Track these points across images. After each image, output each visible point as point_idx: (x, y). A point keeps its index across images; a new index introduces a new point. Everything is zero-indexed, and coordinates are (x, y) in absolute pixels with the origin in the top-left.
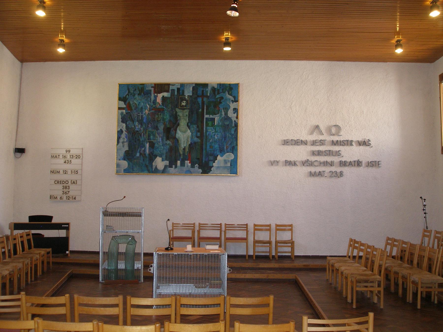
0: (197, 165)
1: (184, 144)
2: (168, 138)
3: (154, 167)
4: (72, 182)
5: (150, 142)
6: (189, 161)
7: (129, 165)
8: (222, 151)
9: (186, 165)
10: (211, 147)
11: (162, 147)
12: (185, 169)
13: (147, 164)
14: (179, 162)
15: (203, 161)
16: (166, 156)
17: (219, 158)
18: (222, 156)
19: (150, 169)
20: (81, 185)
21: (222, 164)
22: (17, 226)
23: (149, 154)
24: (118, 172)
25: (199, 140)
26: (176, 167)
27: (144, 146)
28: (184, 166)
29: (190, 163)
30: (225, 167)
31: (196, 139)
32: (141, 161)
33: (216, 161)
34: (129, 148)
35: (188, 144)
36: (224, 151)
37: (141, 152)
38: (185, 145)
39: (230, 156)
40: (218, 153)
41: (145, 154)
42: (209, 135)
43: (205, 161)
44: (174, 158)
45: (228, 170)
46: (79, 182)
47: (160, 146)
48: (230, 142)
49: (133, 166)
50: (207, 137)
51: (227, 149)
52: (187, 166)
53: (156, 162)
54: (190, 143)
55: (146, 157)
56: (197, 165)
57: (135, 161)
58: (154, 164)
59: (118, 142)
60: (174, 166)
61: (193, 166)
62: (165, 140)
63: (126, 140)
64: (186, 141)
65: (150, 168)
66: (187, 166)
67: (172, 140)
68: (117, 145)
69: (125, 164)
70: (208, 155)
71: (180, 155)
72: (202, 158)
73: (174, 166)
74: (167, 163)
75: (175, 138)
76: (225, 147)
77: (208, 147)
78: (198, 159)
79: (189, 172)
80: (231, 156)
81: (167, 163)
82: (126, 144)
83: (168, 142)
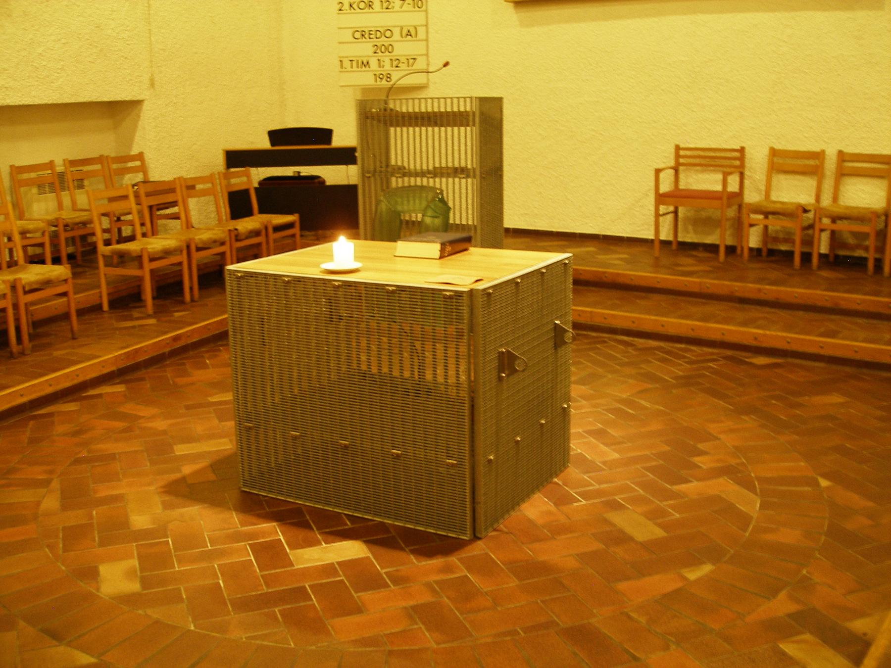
20: (427, 40)
22: (237, 159)
46: (421, 34)
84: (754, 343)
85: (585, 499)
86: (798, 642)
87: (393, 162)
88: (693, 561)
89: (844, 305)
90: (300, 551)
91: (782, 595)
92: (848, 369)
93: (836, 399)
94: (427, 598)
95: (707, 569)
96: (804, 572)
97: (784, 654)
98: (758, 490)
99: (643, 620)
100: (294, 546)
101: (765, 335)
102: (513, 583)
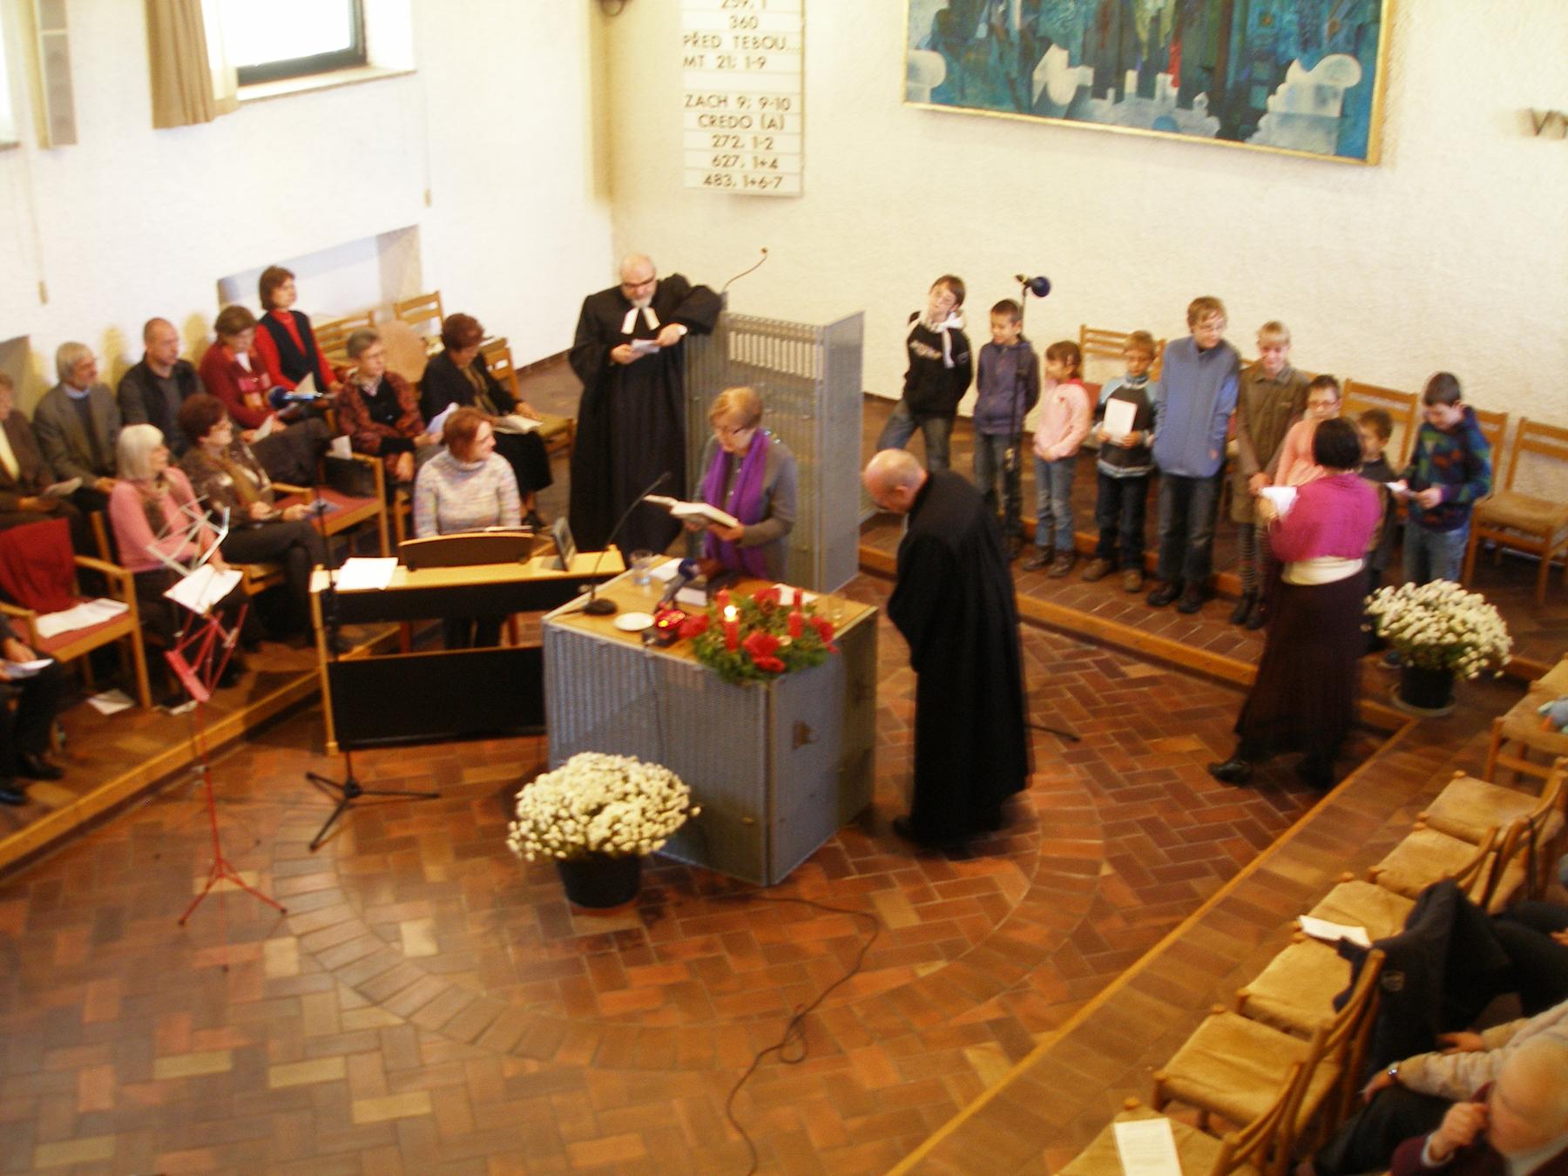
3: (1037, 90)
4: (767, 122)
6: (1170, 78)
7: (949, 71)
8: (1311, 46)
9: (1158, 93)
10: (1264, 15)
12: (1154, 107)
13: (1014, 74)
14: (1131, 78)
15: (1230, 84)
16: (1084, 45)
17: (1295, 73)
18: (1308, 66)
19: (1021, 97)
20: (802, 133)
21: (1306, 106)
23: (1022, 33)
24: (910, 96)
26: (1119, 97)
28: (1151, 95)
30: (1317, 122)
32: (992, 60)
33: (1281, 89)
36: (1319, 45)
37: (995, 20)
38: (1160, 4)
39: (1341, 71)
40: (1292, 52)
41: (1007, 32)
43: (1236, 83)
45: (1329, 133)
48: (1346, 6)
51: (1333, 35)
52: (1164, 98)
53: (1044, 68)
55: (1011, 44)
56: (1201, 97)
57: (972, 56)
58: (1037, 75)
60: (1111, 93)
61: (1185, 101)
65: (1022, 92)
69: (935, 66)
70: (1248, 56)
71: (1138, 46)
72: (1226, 62)
73: (1111, 93)
74: (1085, 75)
76: (1326, 27)
77: (1253, 19)
78: (1209, 70)
79: (1167, 123)
80: (1348, 72)
81: (1085, 75)
87: (732, 356)
90: (580, 918)
91: (993, 1001)
94: (682, 977)
95: (941, 965)
96: (1027, 977)
98: (1034, 875)
100: (575, 913)
102: (760, 966)
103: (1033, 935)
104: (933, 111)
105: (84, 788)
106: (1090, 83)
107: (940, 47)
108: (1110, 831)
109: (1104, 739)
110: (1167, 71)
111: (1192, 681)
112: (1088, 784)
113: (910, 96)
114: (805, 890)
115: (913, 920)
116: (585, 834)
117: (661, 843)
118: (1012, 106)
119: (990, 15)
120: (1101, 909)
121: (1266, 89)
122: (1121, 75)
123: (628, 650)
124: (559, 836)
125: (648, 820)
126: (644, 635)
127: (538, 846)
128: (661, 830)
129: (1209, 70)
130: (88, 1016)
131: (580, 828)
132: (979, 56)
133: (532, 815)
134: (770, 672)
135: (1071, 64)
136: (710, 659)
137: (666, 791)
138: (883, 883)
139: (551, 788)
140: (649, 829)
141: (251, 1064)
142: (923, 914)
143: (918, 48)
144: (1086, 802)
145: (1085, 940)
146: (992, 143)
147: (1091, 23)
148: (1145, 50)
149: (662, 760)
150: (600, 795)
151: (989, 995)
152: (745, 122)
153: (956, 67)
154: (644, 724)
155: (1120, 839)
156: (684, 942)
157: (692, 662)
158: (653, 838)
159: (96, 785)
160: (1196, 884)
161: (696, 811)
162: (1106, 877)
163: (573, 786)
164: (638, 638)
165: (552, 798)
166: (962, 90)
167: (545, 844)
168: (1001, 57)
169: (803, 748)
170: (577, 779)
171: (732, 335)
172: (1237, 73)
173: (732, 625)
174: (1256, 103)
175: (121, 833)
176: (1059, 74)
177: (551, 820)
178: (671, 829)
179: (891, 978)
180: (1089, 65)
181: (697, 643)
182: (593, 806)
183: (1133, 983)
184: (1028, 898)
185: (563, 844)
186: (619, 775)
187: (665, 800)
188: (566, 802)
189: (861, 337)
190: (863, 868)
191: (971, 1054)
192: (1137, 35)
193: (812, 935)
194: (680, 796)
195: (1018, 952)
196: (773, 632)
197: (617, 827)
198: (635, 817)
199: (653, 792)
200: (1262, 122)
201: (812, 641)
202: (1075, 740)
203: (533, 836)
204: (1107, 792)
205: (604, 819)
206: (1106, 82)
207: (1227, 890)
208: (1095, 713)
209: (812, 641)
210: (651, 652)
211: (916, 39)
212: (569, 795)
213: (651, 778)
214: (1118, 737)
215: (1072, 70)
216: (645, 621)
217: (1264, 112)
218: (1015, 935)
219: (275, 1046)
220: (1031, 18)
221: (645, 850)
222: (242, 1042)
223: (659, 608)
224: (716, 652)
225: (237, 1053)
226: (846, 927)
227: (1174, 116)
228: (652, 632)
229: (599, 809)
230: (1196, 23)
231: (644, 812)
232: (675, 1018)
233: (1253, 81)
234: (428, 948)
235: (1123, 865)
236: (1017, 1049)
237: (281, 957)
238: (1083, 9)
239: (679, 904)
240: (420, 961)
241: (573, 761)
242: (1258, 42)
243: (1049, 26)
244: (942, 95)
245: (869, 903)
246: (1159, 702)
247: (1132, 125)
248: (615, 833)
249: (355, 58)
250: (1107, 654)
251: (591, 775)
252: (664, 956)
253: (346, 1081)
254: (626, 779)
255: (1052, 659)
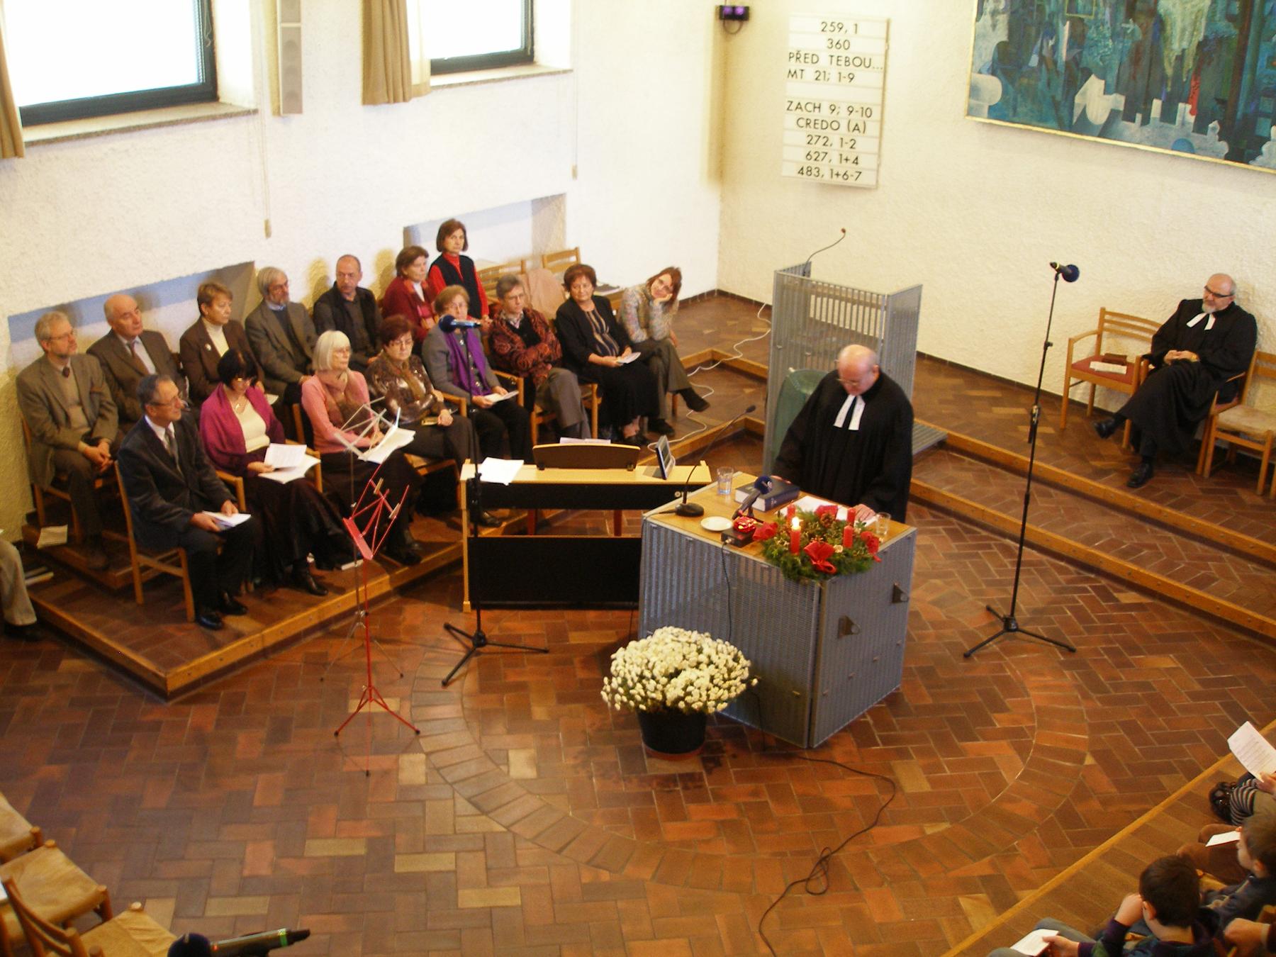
0: (1214, 124)
1: (1181, 39)
2: (1131, 13)
3: (1077, 111)
4: (852, 127)
5: (1071, 19)
6: (1189, 107)
7: (1005, 92)
9: (1178, 119)
11: (1110, 43)
12: (1174, 131)
13: (1059, 97)
14: (1157, 105)
15: (1239, 114)
16: (1118, 77)
24: (971, 112)
25: (1234, 31)
26: (1146, 121)
27: (1053, 32)
28: (1173, 121)
29: (1192, 112)
31: (1223, 26)
32: (1041, 85)
34: (1010, 34)
35: (1195, 43)
37: (1044, 52)
38: (1185, 44)
41: (1055, 63)
42: (1271, 13)
43: (1245, 115)
44: (1145, 86)
47: (1104, 37)
49: (1015, 99)
50: (1263, 21)
52: (1183, 124)
53: (1084, 93)
54: (1201, 38)
56: (1214, 124)
57: (1025, 81)
58: (1078, 99)
59: (980, 12)
60: (1139, 117)
61: (1200, 127)
62: (1121, 16)
63: (1001, 7)
64: (1190, 29)
65: (1064, 113)
66: (1183, 124)
67: (1142, 19)
68: (977, 20)
69: (993, 87)
71: (1164, 78)
72: (1238, 95)
73: (1139, 117)
74: (1118, 101)
75: (1153, 12)
77: (1262, 61)
78: (1222, 102)
79: (1185, 145)
81: (1118, 101)
82: (1003, 19)
83: (1131, 26)
84: (1127, 578)
85: (884, 744)
86: (976, 899)
88: (935, 818)
89: (1237, 545)
90: (653, 760)
92: (1207, 624)
93: (1167, 662)
94: (734, 816)
95: (945, 826)
97: (959, 905)
99: (875, 860)
100: (649, 756)
101: (1138, 572)
102: (799, 813)
103: (1024, 809)
104: (991, 124)
105: (270, 621)
106: (1122, 109)
107: (999, 72)
108: (1094, 729)
109: (1097, 652)
110: (1186, 102)
111: (1172, 609)
112: (1079, 687)
113: (971, 112)
114: (838, 754)
115: (926, 787)
116: (663, 693)
117: (725, 705)
118: (1055, 124)
119: (1042, 47)
120: (1082, 793)
121: (1269, 121)
122: (1148, 103)
123: (709, 546)
124: (643, 693)
125: (716, 685)
126: (724, 535)
127: (625, 699)
128: (726, 695)
129: (1222, 102)
130: (257, 801)
131: (659, 687)
132: (1030, 81)
133: (622, 674)
134: (824, 573)
135: (1106, 92)
136: (776, 560)
137: (731, 663)
138: (903, 754)
139: (639, 653)
140: (715, 693)
141: (382, 852)
142: (933, 782)
143: (980, 72)
144: (1079, 703)
145: (1067, 816)
146: (1038, 155)
147: (1125, 59)
148: (1170, 84)
149: (730, 638)
150: (679, 661)
151: (980, 854)
152: (835, 125)
153: (1010, 87)
154: (718, 608)
155: (1103, 736)
156: (736, 788)
157: (761, 560)
158: (718, 701)
159: (279, 619)
160: (1164, 780)
161: (755, 681)
162: (1090, 766)
163: (656, 653)
164: (719, 537)
165: (639, 661)
166: (1015, 109)
167: (631, 697)
168: (1049, 84)
169: (846, 638)
170: (660, 648)
171: (813, 297)
172: (1247, 105)
173: (796, 534)
174: (1261, 132)
175: (295, 658)
176: (1096, 99)
177: (636, 679)
178: (733, 694)
179: (905, 832)
180: (1121, 94)
181: (767, 546)
182: (672, 671)
183: (1104, 856)
184: (1020, 778)
185: (645, 699)
186: (694, 647)
187: (730, 671)
188: (650, 665)
189: (919, 307)
190: (886, 741)
191: (965, 902)
192: (1164, 69)
193: (841, 792)
194: (742, 669)
195: (1009, 821)
196: (829, 540)
197: (690, 688)
198: (705, 682)
199: (721, 664)
200: (1264, 148)
201: (860, 551)
202: (1072, 650)
203: (621, 690)
204: (1094, 696)
205: (680, 681)
206: (1135, 108)
207: (1189, 786)
208: (1089, 630)
209: (860, 551)
210: (728, 549)
211: (979, 64)
212: (653, 660)
213: (721, 651)
214: (1107, 651)
215: (1107, 97)
216: (727, 524)
217: (1268, 139)
218: (1008, 807)
219: (402, 839)
220: (1076, 51)
221: (711, 710)
222: (374, 833)
223: (738, 515)
224: (781, 553)
225: (371, 842)
226: (870, 788)
227: (1190, 139)
228: (731, 533)
229: (677, 673)
230: (1214, 63)
231: (712, 678)
232: (723, 848)
233: (1259, 114)
234: (530, 773)
235: (1103, 757)
236: (1002, 901)
237: (413, 769)
238: (1120, 46)
239: (734, 756)
240: (522, 782)
241: (658, 632)
242: (1265, 81)
243: (1089, 59)
244: (996, 112)
245: (891, 770)
246: (1144, 624)
247: (1155, 145)
248: (690, 694)
249: (524, 57)
250: (1104, 582)
251: (672, 645)
252: (718, 797)
253: (455, 872)
254: (700, 651)
255: (1058, 582)
